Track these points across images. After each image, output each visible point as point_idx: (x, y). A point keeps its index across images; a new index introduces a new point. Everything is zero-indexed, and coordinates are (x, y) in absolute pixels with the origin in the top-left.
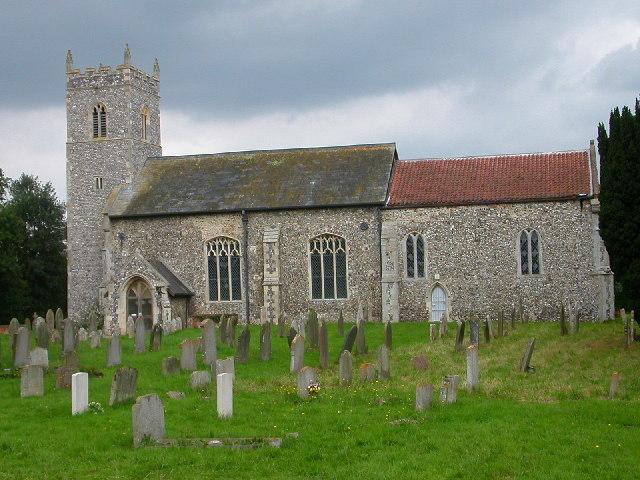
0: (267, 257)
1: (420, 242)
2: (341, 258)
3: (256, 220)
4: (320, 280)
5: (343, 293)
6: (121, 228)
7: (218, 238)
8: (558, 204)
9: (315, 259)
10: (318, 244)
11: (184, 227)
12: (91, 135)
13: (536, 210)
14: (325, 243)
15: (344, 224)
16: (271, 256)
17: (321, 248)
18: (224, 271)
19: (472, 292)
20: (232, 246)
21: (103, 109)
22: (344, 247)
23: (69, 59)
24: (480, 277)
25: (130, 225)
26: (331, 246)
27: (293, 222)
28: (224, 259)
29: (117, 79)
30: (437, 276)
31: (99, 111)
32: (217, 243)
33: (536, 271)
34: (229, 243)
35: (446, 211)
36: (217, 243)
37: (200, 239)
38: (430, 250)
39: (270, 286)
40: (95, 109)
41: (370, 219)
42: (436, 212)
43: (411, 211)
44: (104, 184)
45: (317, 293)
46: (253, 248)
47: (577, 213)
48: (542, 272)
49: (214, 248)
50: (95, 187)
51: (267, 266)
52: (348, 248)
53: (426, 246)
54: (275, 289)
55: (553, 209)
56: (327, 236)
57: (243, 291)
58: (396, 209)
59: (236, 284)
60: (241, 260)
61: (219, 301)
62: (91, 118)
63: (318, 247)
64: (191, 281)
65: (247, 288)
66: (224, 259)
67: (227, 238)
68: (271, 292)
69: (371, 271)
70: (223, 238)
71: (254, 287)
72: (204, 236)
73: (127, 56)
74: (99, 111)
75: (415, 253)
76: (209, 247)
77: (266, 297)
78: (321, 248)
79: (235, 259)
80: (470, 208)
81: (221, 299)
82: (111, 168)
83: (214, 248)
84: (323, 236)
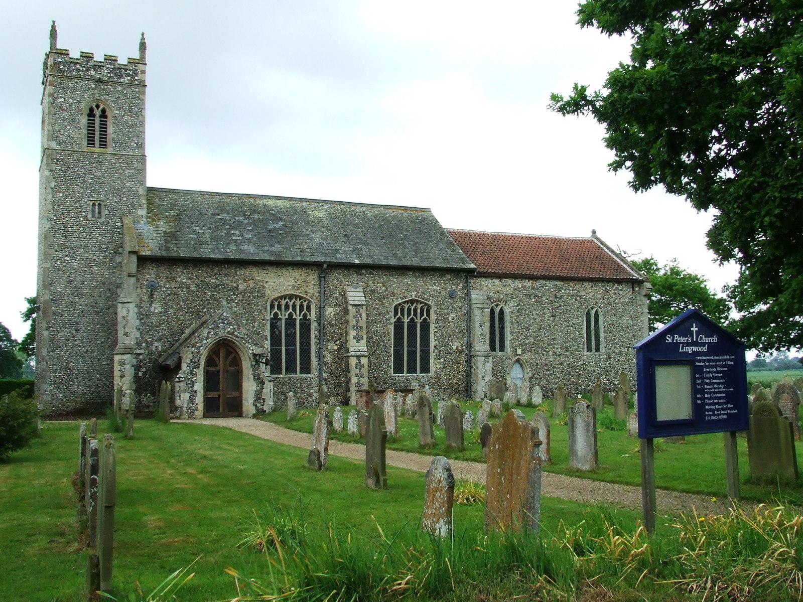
0: (353, 322)
1: (502, 312)
2: (425, 326)
3: (335, 278)
5: (425, 369)
6: (150, 274)
7: (284, 297)
8: (616, 285)
9: (399, 326)
10: (402, 310)
11: (241, 280)
12: (84, 142)
13: (599, 289)
15: (432, 289)
16: (358, 321)
17: (406, 317)
18: (291, 338)
19: (547, 368)
20: (301, 306)
21: (104, 111)
22: (428, 314)
23: (53, 34)
24: (555, 354)
25: (164, 272)
26: (415, 314)
27: (378, 283)
28: (290, 322)
29: (128, 75)
30: (519, 351)
31: (98, 113)
32: (283, 302)
33: (597, 349)
34: (298, 303)
35: (528, 283)
36: (283, 302)
37: (263, 296)
38: (512, 323)
39: (358, 357)
40: (91, 110)
41: (458, 286)
42: (518, 284)
43: (497, 281)
44: (105, 212)
45: (398, 369)
46: (330, 311)
47: (630, 295)
49: (279, 307)
50: (90, 215)
51: (352, 333)
52: (433, 317)
53: (507, 318)
54: (364, 361)
55: (613, 288)
56: (412, 302)
58: (484, 277)
59: (306, 353)
61: (283, 375)
62: (84, 120)
63: (402, 314)
65: (320, 356)
66: (290, 322)
67: (296, 297)
68: (359, 365)
69: (457, 344)
70: (291, 297)
72: (268, 292)
73: (143, 47)
74: (98, 113)
76: (272, 306)
77: (354, 370)
78: (406, 317)
79: (306, 326)
80: (548, 283)
81: (287, 373)
82: (116, 192)
83: (279, 307)
84: (407, 302)
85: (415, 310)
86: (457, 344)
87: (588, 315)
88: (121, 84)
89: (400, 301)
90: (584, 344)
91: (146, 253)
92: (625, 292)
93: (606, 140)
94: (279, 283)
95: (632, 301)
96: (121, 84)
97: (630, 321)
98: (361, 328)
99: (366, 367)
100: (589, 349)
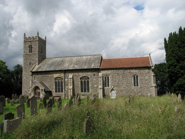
0: (69, 82)
2: (88, 82)
4: (84, 84)
5: (89, 91)
9: (81, 82)
14: (84, 78)
15: (89, 74)
18: (59, 85)
19: (121, 91)
20: (61, 79)
23: (25, 35)
31: (31, 47)
33: (138, 85)
39: (70, 89)
45: (82, 91)
46: (66, 80)
48: (139, 86)
51: (69, 84)
54: (71, 90)
56: (85, 77)
57: (64, 91)
60: (63, 83)
64: (51, 88)
69: (96, 86)
71: (66, 89)
75: (105, 83)
77: (69, 92)
79: (62, 82)
82: (33, 60)
85: (86, 78)
86: (96, 86)
87: (134, 76)
88: (34, 41)
89: (81, 77)
90: (133, 84)
91: (33, 71)
92: (147, 71)
93: (171, 33)
94: (56, 75)
95: (149, 73)
96: (34, 41)
97: (148, 78)
98: (71, 83)
99: (72, 91)
100: (135, 86)
